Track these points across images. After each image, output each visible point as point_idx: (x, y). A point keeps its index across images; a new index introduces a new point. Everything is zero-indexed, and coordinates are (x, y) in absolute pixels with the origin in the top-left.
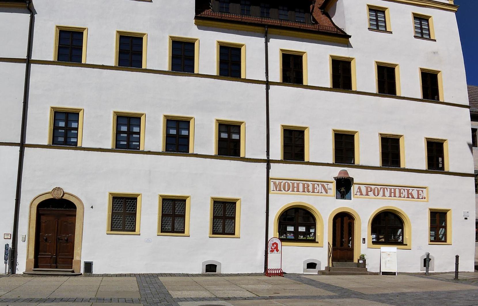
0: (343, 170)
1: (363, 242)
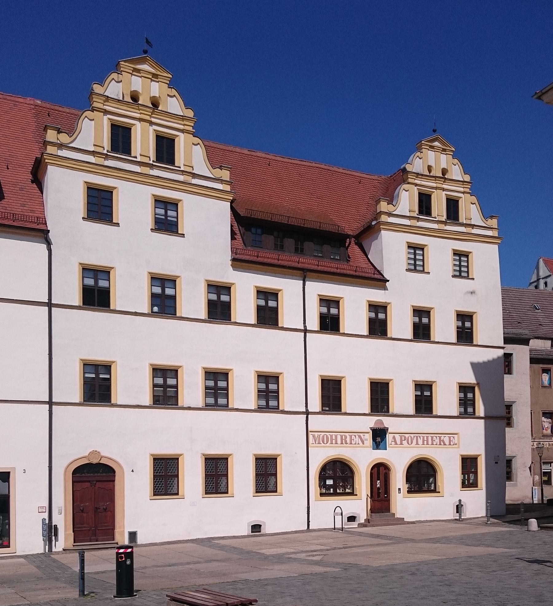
0: (378, 420)
1: (399, 492)
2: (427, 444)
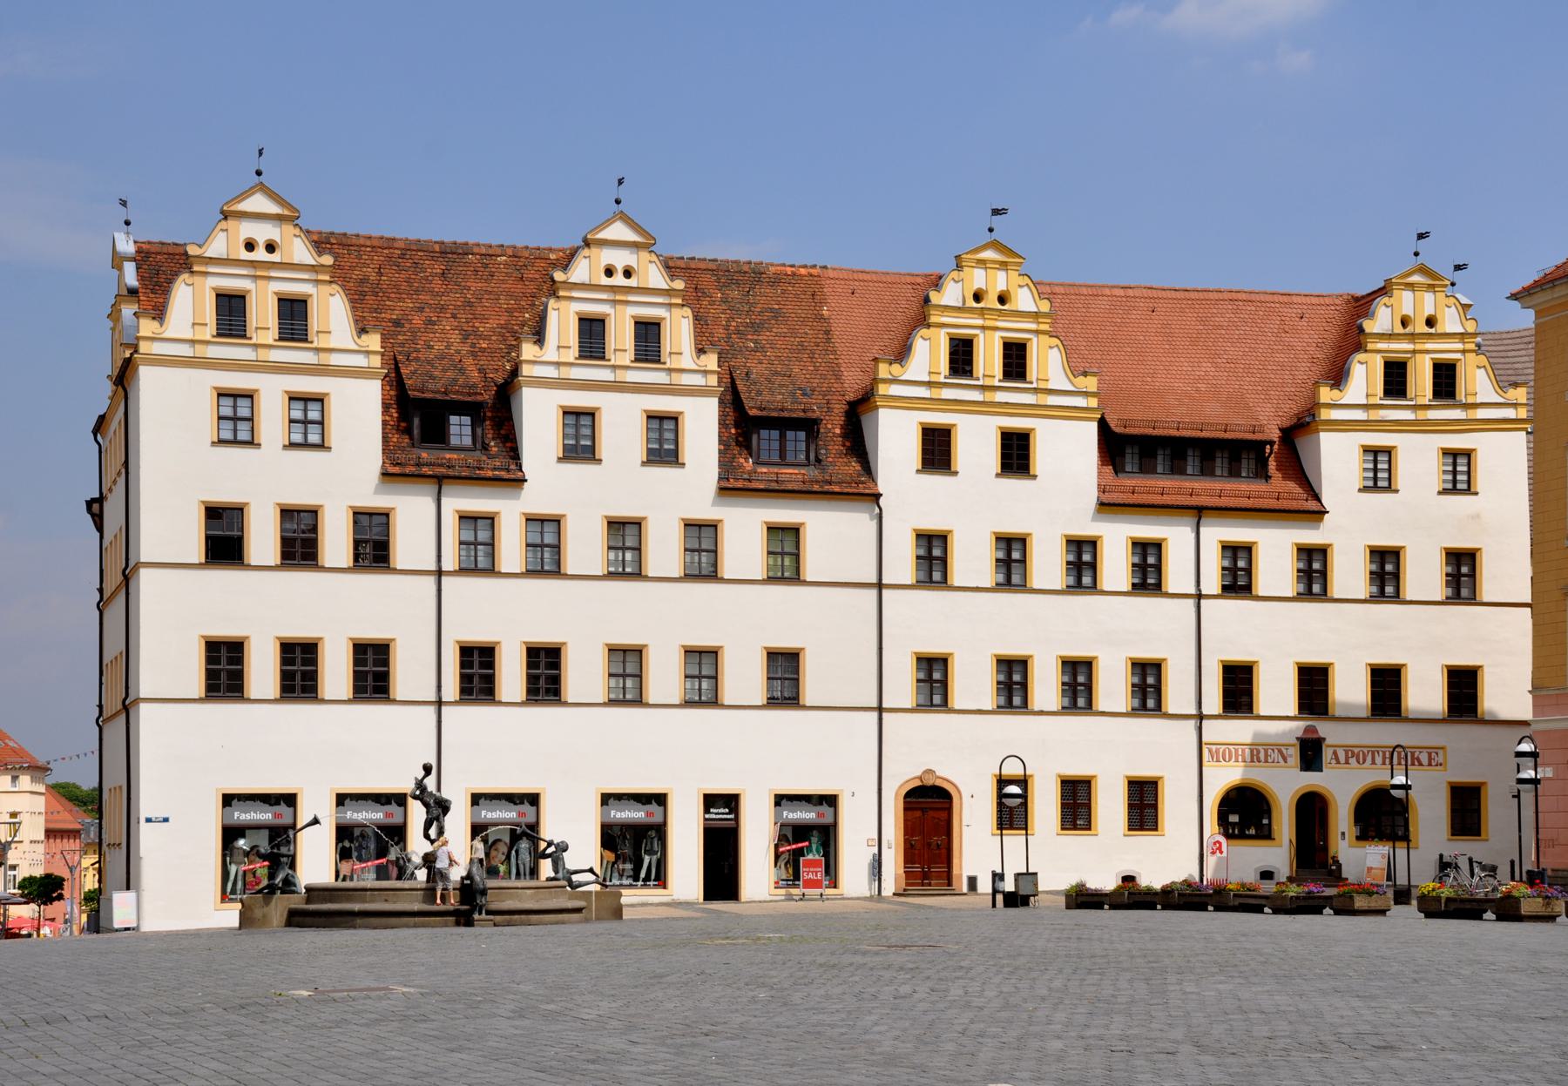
0: (1308, 726)
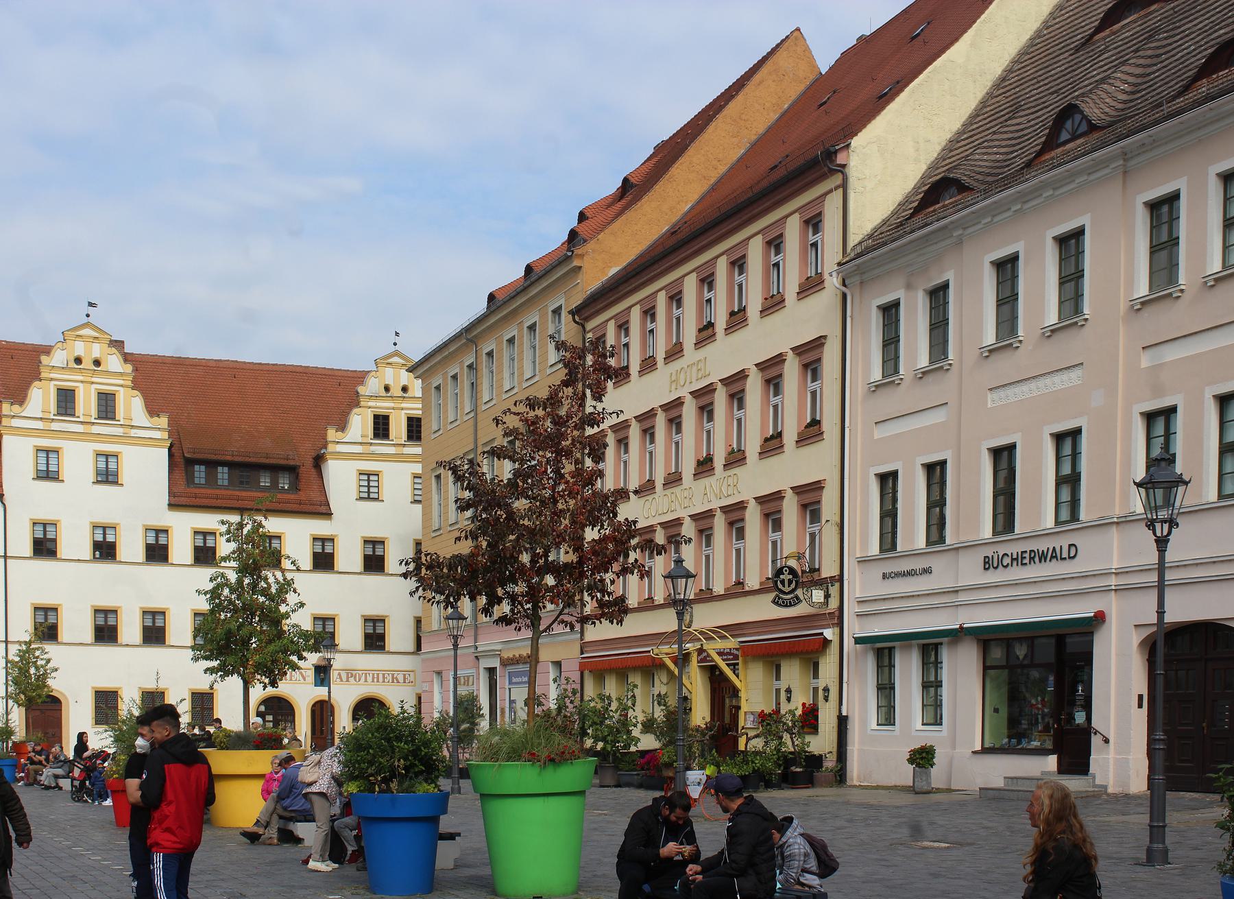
2: (378, 681)
